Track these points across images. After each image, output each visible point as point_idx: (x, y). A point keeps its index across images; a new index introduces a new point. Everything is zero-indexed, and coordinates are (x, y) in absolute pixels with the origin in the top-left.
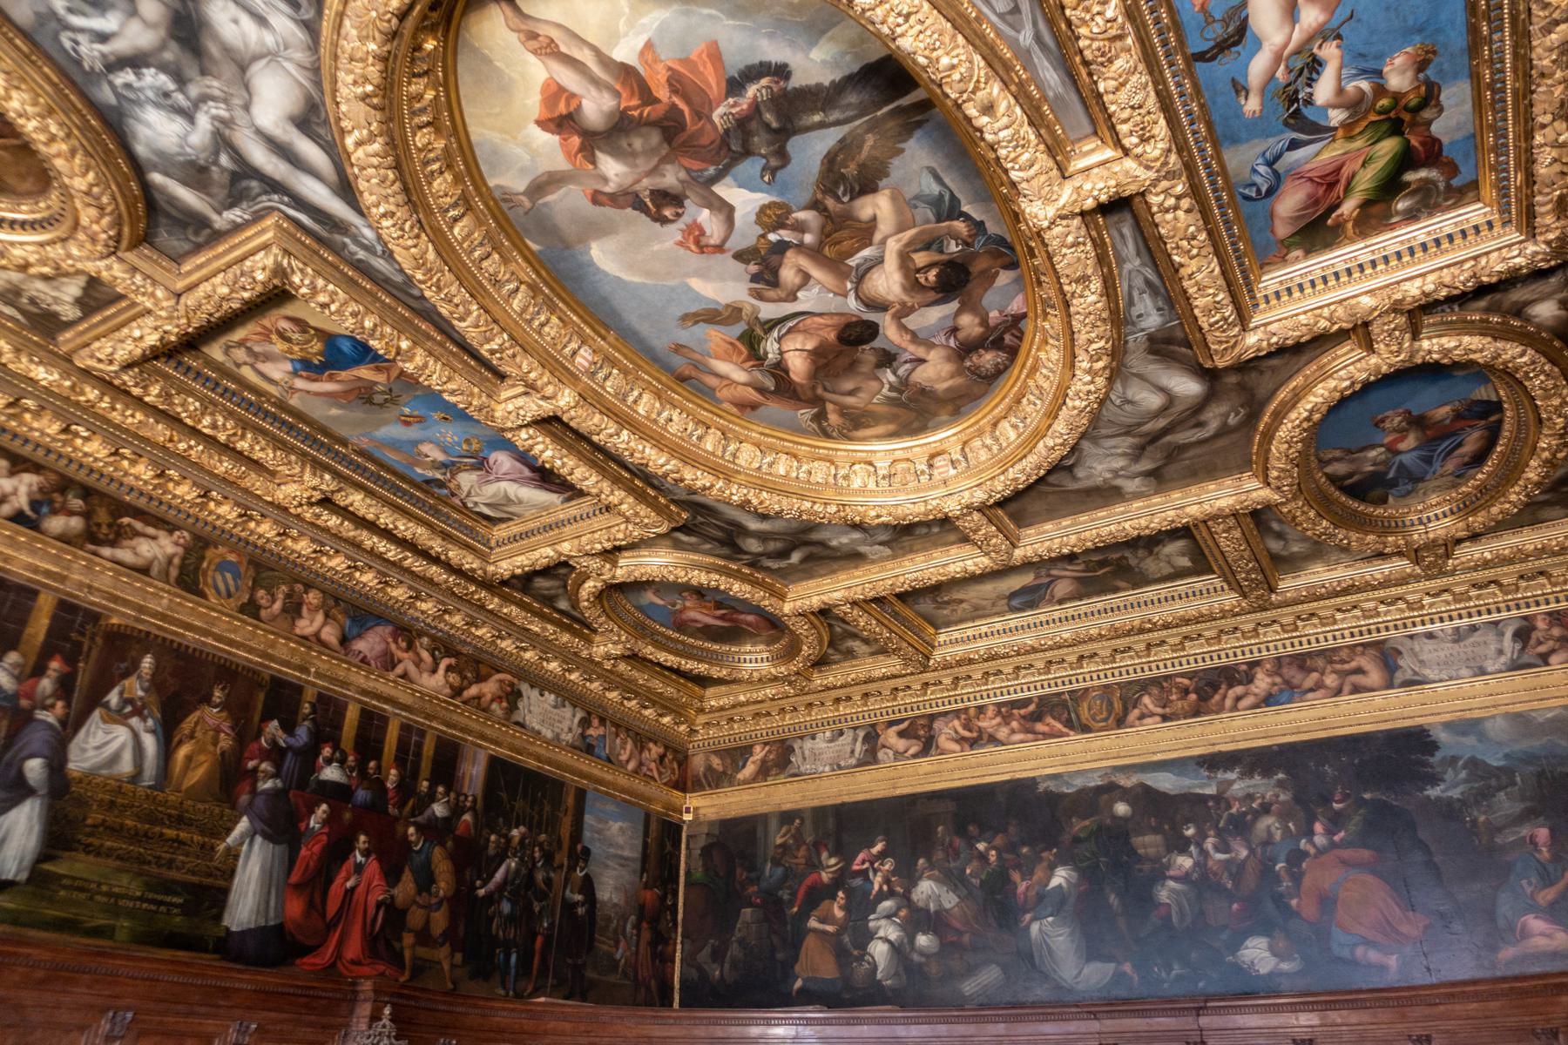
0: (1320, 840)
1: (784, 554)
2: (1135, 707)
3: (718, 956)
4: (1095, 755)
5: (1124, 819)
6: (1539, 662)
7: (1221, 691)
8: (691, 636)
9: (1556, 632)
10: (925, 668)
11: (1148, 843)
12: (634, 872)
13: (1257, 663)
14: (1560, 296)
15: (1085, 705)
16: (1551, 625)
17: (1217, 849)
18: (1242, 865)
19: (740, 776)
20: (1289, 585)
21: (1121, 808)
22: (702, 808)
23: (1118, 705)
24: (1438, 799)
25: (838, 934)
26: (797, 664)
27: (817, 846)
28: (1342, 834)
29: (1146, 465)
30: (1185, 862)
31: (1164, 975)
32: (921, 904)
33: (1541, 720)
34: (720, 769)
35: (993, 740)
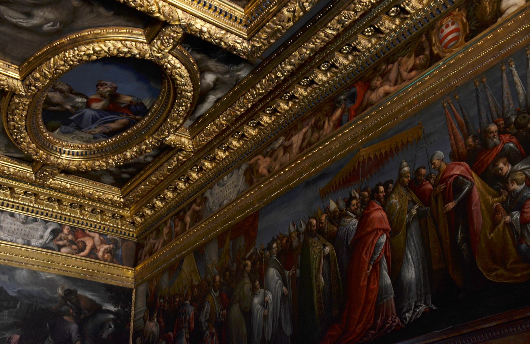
6: (56, 248)
9: (70, 237)
14: (220, 76)
16: (69, 233)
33: (44, 278)
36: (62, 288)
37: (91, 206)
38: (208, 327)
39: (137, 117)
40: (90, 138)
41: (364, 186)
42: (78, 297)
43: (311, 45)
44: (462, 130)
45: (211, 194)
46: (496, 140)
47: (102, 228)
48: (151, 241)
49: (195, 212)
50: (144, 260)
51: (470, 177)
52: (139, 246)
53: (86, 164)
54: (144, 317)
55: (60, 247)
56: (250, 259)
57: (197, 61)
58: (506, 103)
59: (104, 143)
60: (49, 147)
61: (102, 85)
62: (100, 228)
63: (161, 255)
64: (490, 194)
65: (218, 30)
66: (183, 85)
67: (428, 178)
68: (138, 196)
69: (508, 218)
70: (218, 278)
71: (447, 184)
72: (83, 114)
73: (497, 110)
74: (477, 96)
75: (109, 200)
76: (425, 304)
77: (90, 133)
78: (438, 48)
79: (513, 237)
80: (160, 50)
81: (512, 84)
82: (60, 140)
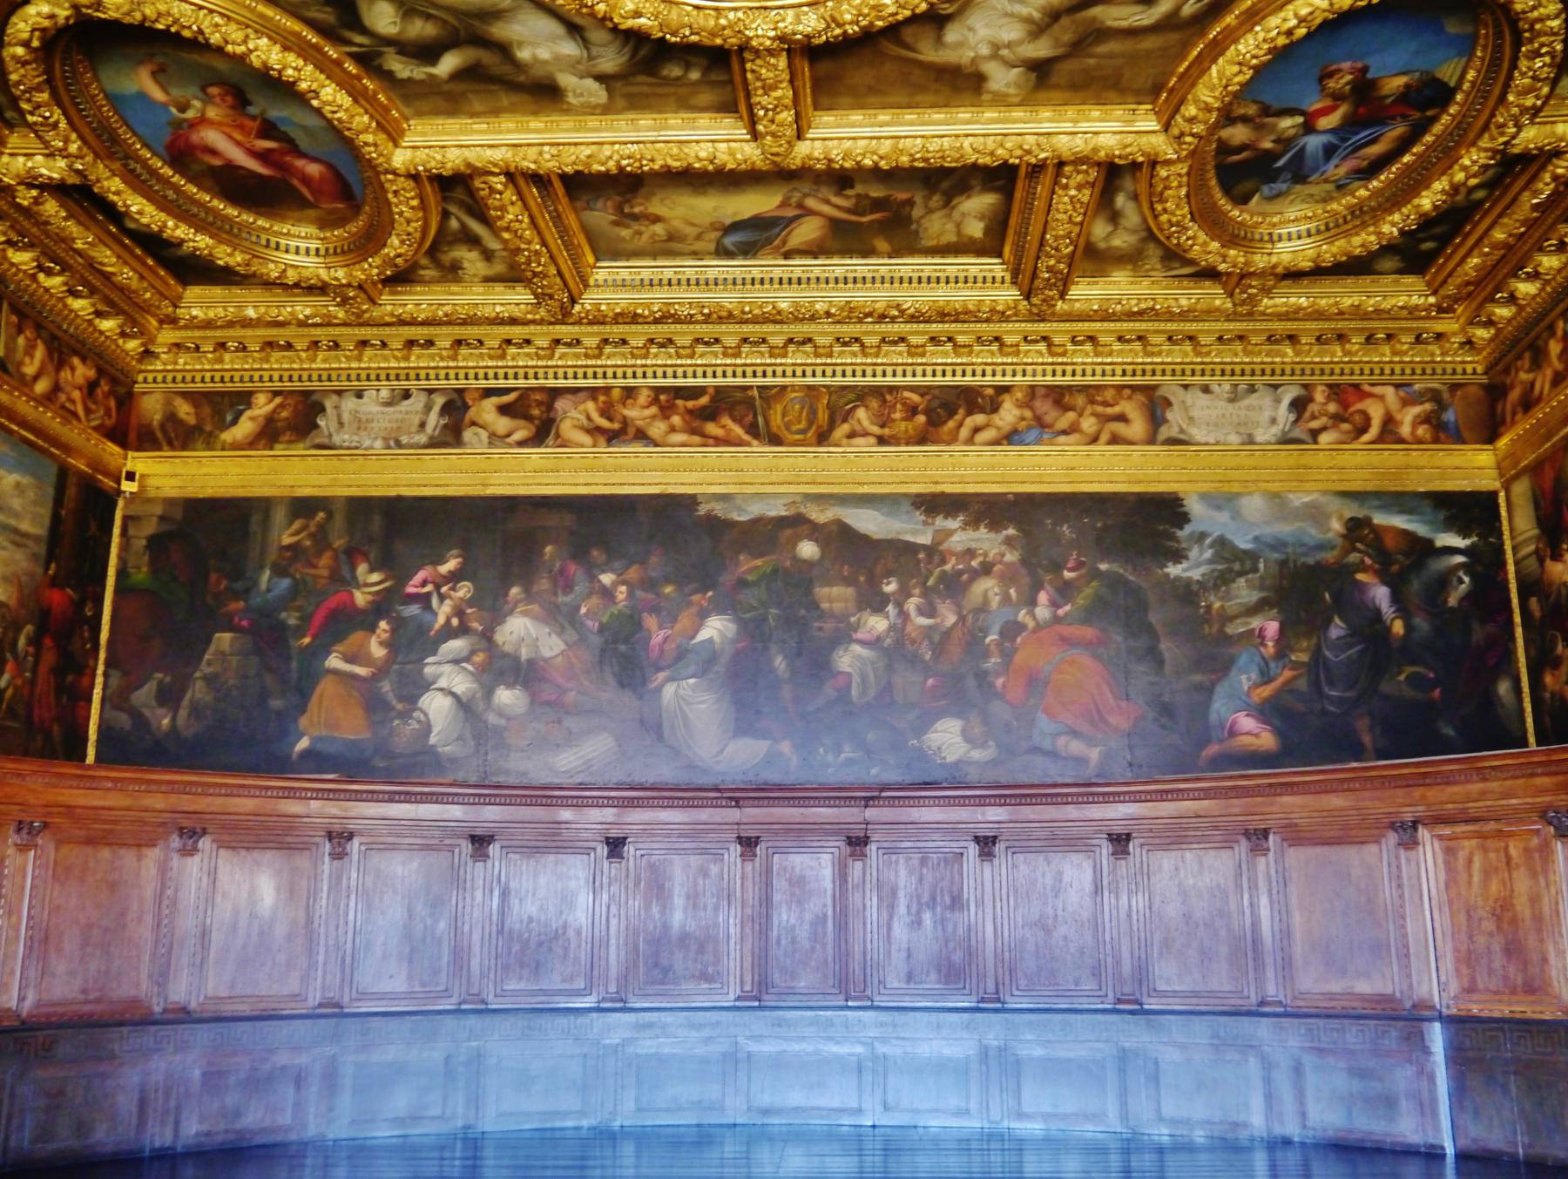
0: (1043, 612)
1: (428, 52)
2: (845, 420)
3: (169, 697)
4: (782, 476)
5: (810, 564)
7: (958, 417)
8: (190, 180)
9: (1332, 408)
10: (564, 317)
11: (835, 596)
12: (35, 557)
13: (1005, 389)
15: (779, 408)
16: (1329, 399)
17: (921, 612)
18: (947, 634)
19: (227, 436)
20: (1086, 292)
21: (808, 549)
22: (161, 476)
23: (823, 416)
24: (1178, 579)
25: (374, 678)
26: (371, 268)
27: (352, 554)
28: (1068, 608)
29: (1041, 49)
30: (877, 624)
31: (830, 757)
32: (508, 648)
33: (1297, 503)
34: (192, 421)
35: (642, 436)
36: (1340, 517)
37: (1362, 330)
39: (1429, 113)
42: (1378, 532)
47: (1398, 371)
50: (1513, 423)
52: (1495, 391)
53: (1332, 251)
54: (1537, 552)
55: (1315, 434)
59: (1362, 193)
60: (1245, 237)
61: (1330, 75)
62: (1393, 372)
63: (1552, 408)
66: (1534, 8)
68: (1468, 283)
72: (1303, 149)
75: (1402, 308)
77: (1326, 181)
82: (1264, 215)
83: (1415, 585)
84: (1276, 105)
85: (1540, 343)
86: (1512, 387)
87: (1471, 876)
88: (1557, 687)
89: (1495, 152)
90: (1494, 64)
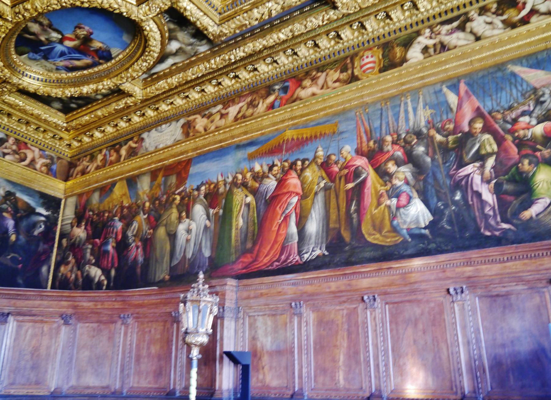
9: (14, 147)
14: (183, 46)
16: (14, 144)
36: (4, 189)
37: (36, 124)
38: (134, 241)
39: (101, 61)
40: (52, 69)
41: (285, 159)
42: (17, 199)
43: (265, 43)
44: (367, 135)
45: (148, 136)
46: (389, 148)
47: (42, 144)
48: (85, 163)
49: (131, 148)
50: (75, 178)
51: (367, 169)
52: (72, 165)
53: (43, 89)
54: (71, 223)
56: (179, 194)
57: (170, 30)
58: (400, 124)
59: (64, 75)
60: (14, 68)
61: (80, 28)
62: (40, 144)
64: (379, 183)
65: (198, 11)
66: (154, 46)
67: (336, 163)
68: (80, 125)
69: (388, 202)
70: (147, 204)
71: (349, 170)
72: (54, 48)
73: (393, 127)
74: (381, 114)
75: (54, 123)
76: (320, 249)
77: (54, 64)
78: (359, 71)
79: (389, 215)
80: (146, 14)
81: (406, 112)
82: (24, 64)
83: (24, 224)
84: (55, 26)
85: (95, 154)
86: (79, 165)
87: (25, 337)
88: (65, 272)
89: (116, 85)
90: (131, 57)
